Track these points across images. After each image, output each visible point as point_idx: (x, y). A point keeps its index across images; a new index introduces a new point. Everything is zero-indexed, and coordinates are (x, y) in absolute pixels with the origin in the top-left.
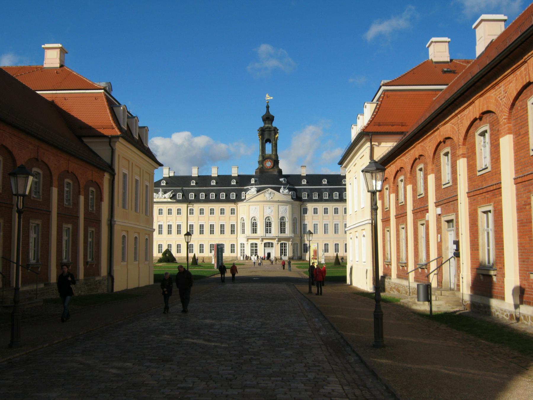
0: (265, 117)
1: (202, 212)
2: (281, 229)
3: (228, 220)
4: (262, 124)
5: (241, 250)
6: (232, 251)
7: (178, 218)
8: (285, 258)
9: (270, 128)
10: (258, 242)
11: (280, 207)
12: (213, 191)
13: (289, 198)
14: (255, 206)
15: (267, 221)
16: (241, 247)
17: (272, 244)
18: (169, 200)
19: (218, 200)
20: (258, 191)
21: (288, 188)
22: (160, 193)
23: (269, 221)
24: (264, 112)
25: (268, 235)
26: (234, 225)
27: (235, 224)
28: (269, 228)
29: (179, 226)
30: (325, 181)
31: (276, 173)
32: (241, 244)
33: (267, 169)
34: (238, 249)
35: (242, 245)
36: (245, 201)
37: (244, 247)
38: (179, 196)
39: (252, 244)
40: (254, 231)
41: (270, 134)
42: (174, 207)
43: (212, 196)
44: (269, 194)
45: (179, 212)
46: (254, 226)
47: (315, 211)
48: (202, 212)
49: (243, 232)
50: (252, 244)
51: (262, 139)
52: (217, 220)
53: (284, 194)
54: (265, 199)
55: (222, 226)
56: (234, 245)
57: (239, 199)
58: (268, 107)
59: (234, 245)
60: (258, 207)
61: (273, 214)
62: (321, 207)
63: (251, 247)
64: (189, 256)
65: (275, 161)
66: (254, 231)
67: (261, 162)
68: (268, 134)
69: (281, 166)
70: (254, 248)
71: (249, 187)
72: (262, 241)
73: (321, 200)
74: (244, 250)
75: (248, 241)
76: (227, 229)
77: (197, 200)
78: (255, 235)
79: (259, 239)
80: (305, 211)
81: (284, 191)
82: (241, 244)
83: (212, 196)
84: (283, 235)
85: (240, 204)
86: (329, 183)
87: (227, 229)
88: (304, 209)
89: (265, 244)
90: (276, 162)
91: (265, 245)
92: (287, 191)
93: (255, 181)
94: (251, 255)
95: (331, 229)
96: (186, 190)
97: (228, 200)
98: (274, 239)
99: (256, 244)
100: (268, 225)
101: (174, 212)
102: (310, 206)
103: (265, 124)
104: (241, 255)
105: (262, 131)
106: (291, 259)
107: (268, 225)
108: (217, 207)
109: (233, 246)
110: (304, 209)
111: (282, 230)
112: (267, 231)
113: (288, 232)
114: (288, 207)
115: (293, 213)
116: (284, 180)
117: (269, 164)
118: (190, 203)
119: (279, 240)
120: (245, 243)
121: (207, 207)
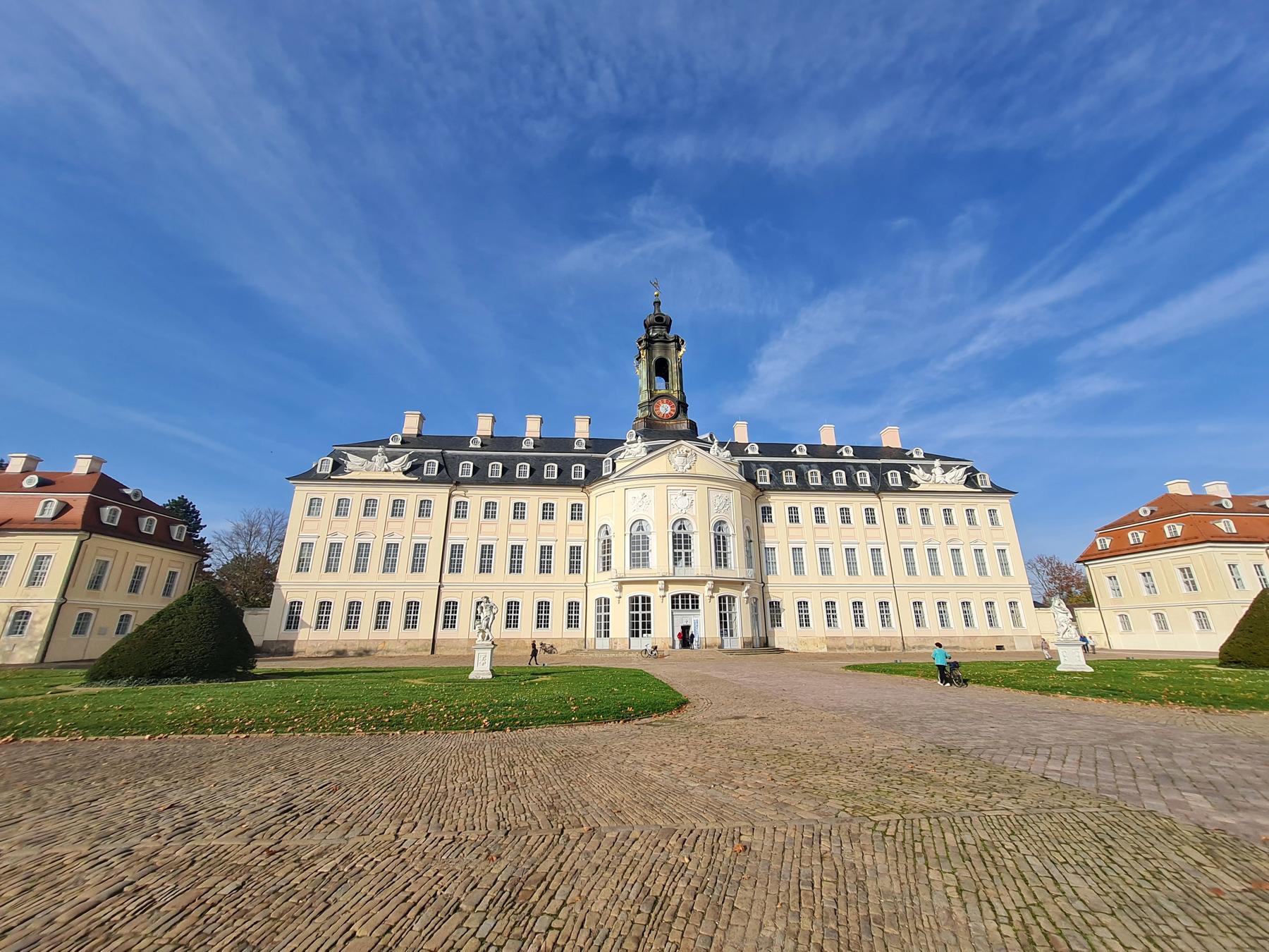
0: (652, 319)
1: (490, 510)
3: (562, 534)
5: (599, 618)
6: (572, 622)
8: (735, 643)
10: (653, 592)
11: (713, 494)
12: (525, 459)
13: (734, 473)
14: (643, 491)
16: (599, 610)
17: (695, 599)
19: (536, 479)
20: (650, 450)
22: (378, 459)
23: (682, 532)
24: (648, 312)
25: (682, 572)
27: (583, 545)
28: (683, 551)
29: (420, 550)
31: (684, 426)
32: (599, 601)
33: (662, 420)
34: (589, 616)
35: (604, 604)
37: (607, 609)
38: (432, 467)
39: (634, 600)
41: (666, 349)
42: (412, 495)
43: (523, 471)
44: (678, 456)
45: (424, 509)
46: (639, 547)
47: (793, 515)
48: (490, 510)
49: (607, 565)
50: (634, 600)
51: (650, 357)
52: (531, 534)
53: (715, 462)
54: (672, 471)
56: (577, 604)
57: (594, 475)
59: (577, 604)
60: (650, 493)
61: (694, 511)
62: (805, 503)
63: (632, 608)
64: (438, 637)
65: (679, 403)
69: (690, 416)
70: (640, 612)
71: (620, 448)
72: (666, 589)
73: (803, 486)
74: (607, 618)
75: (621, 590)
76: (560, 560)
77: (480, 478)
78: (640, 573)
79: (656, 582)
80: (767, 511)
82: (599, 601)
83: (523, 471)
85: (598, 490)
87: (560, 560)
89: (674, 599)
90: (682, 406)
92: (728, 453)
95: (837, 560)
96: (454, 457)
97: (564, 480)
98: (704, 582)
99: (647, 600)
100: (681, 542)
101: (411, 508)
102: (779, 503)
104: (598, 635)
106: (749, 645)
108: (534, 498)
109: (573, 607)
111: (721, 559)
113: (737, 567)
114: (734, 496)
117: (665, 409)
118: (457, 484)
119: (718, 583)
121: (505, 498)
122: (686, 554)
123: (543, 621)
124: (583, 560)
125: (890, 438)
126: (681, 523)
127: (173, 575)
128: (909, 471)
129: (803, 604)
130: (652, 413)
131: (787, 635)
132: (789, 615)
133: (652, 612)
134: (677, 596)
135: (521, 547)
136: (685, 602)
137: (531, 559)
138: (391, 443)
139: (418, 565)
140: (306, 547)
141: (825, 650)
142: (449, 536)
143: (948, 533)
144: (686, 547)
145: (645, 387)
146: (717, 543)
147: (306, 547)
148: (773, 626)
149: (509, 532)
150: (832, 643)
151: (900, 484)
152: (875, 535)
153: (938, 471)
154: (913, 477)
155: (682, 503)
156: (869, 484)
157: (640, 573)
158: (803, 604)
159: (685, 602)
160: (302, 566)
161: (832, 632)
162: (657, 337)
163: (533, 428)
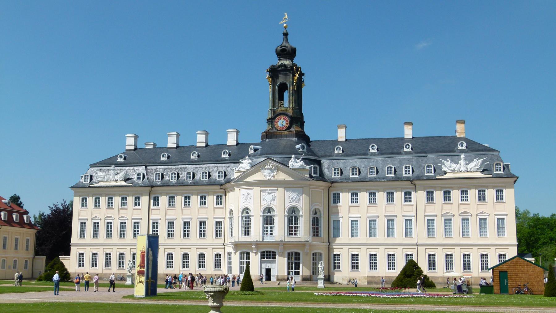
2: (290, 229)
4: (276, 62)
6: (218, 265)
7: (136, 212)
9: (285, 66)
15: (266, 214)
18: (124, 183)
21: (303, 159)
24: (279, 41)
26: (221, 222)
28: (269, 226)
29: (136, 224)
30: (373, 150)
36: (233, 183)
40: (247, 231)
55: (202, 224)
58: (286, 35)
63: (241, 258)
65: (291, 118)
66: (247, 231)
67: (271, 121)
68: (286, 78)
76: (210, 229)
81: (296, 163)
82: (229, 253)
84: (293, 239)
86: (381, 152)
87: (210, 229)
88: (334, 194)
91: (263, 256)
92: (302, 163)
93: (255, 150)
94: (241, 273)
100: (268, 221)
103: (280, 60)
105: (274, 72)
107: (268, 221)
109: (218, 256)
110: (334, 194)
112: (265, 232)
115: (311, 203)
116: (302, 147)
117: (282, 123)
118: (152, 187)
120: (232, 251)
122: (271, 228)
123: (201, 264)
124: (223, 230)
125: (460, 130)
126: (269, 209)
127: (28, 240)
128: (441, 162)
129: (355, 256)
130: (273, 126)
131: (343, 275)
132: (345, 261)
133: (250, 261)
134: (264, 252)
135: (189, 222)
136: (268, 255)
137: (194, 229)
138: (119, 160)
139: (136, 232)
140: (83, 224)
141: (366, 283)
142: (151, 217)
143: (462, 207)
144: (271, 224)
145: (270, 108)
146: (290, 222)
147: (83, 224)
148: (335, 268)
149: (182, 214)
150: (370, 279)
151: (432, 174)
152: (409, 211)
153: (462, 162)
154: (444, 169)
155: (269, 197)
156: (411, 175)
157: (247, 239)
158: (355, 256)
159: (268, 255)
160: (82, 234)
161: (373, 273)
162: (280, 66)
163: (201, 141)
